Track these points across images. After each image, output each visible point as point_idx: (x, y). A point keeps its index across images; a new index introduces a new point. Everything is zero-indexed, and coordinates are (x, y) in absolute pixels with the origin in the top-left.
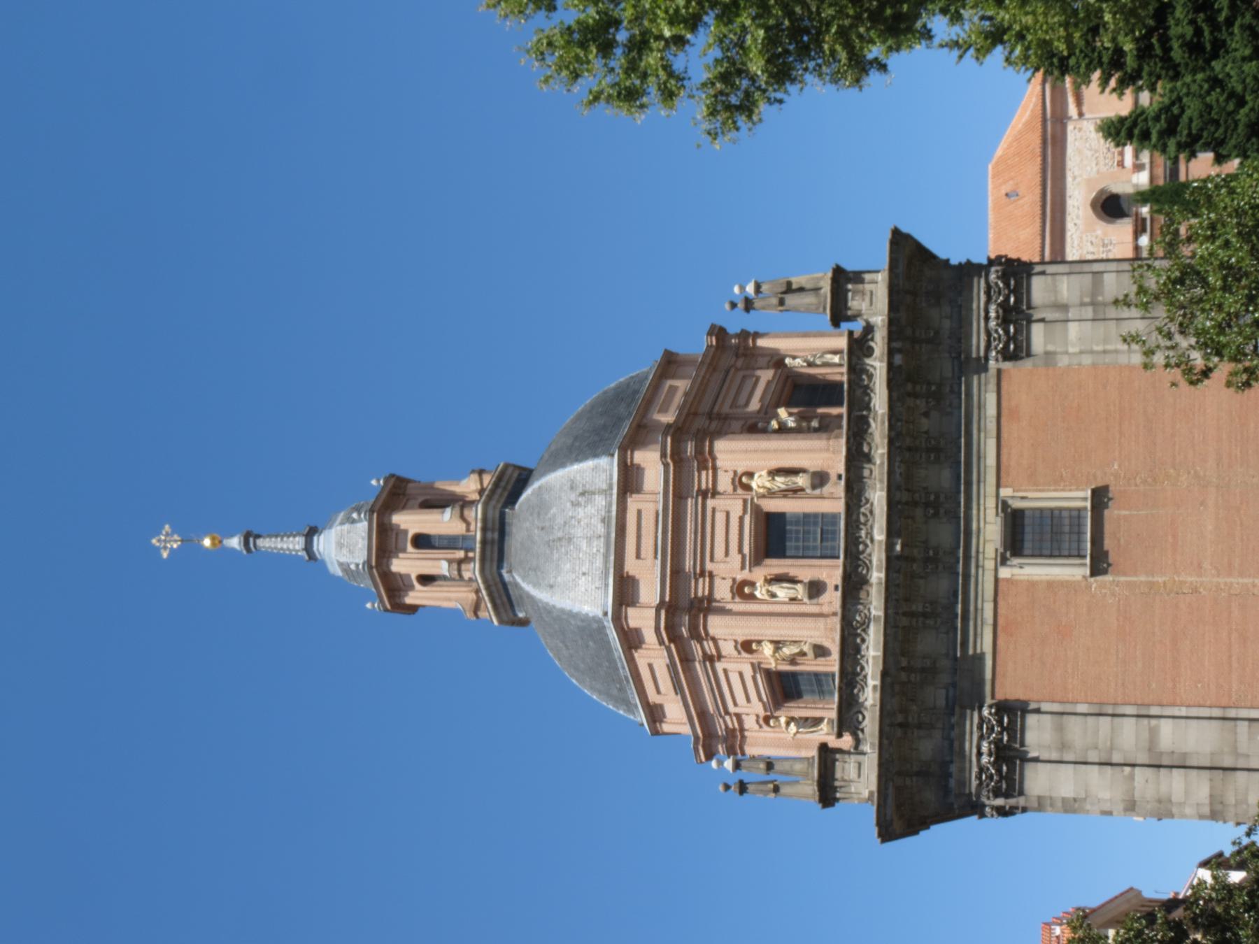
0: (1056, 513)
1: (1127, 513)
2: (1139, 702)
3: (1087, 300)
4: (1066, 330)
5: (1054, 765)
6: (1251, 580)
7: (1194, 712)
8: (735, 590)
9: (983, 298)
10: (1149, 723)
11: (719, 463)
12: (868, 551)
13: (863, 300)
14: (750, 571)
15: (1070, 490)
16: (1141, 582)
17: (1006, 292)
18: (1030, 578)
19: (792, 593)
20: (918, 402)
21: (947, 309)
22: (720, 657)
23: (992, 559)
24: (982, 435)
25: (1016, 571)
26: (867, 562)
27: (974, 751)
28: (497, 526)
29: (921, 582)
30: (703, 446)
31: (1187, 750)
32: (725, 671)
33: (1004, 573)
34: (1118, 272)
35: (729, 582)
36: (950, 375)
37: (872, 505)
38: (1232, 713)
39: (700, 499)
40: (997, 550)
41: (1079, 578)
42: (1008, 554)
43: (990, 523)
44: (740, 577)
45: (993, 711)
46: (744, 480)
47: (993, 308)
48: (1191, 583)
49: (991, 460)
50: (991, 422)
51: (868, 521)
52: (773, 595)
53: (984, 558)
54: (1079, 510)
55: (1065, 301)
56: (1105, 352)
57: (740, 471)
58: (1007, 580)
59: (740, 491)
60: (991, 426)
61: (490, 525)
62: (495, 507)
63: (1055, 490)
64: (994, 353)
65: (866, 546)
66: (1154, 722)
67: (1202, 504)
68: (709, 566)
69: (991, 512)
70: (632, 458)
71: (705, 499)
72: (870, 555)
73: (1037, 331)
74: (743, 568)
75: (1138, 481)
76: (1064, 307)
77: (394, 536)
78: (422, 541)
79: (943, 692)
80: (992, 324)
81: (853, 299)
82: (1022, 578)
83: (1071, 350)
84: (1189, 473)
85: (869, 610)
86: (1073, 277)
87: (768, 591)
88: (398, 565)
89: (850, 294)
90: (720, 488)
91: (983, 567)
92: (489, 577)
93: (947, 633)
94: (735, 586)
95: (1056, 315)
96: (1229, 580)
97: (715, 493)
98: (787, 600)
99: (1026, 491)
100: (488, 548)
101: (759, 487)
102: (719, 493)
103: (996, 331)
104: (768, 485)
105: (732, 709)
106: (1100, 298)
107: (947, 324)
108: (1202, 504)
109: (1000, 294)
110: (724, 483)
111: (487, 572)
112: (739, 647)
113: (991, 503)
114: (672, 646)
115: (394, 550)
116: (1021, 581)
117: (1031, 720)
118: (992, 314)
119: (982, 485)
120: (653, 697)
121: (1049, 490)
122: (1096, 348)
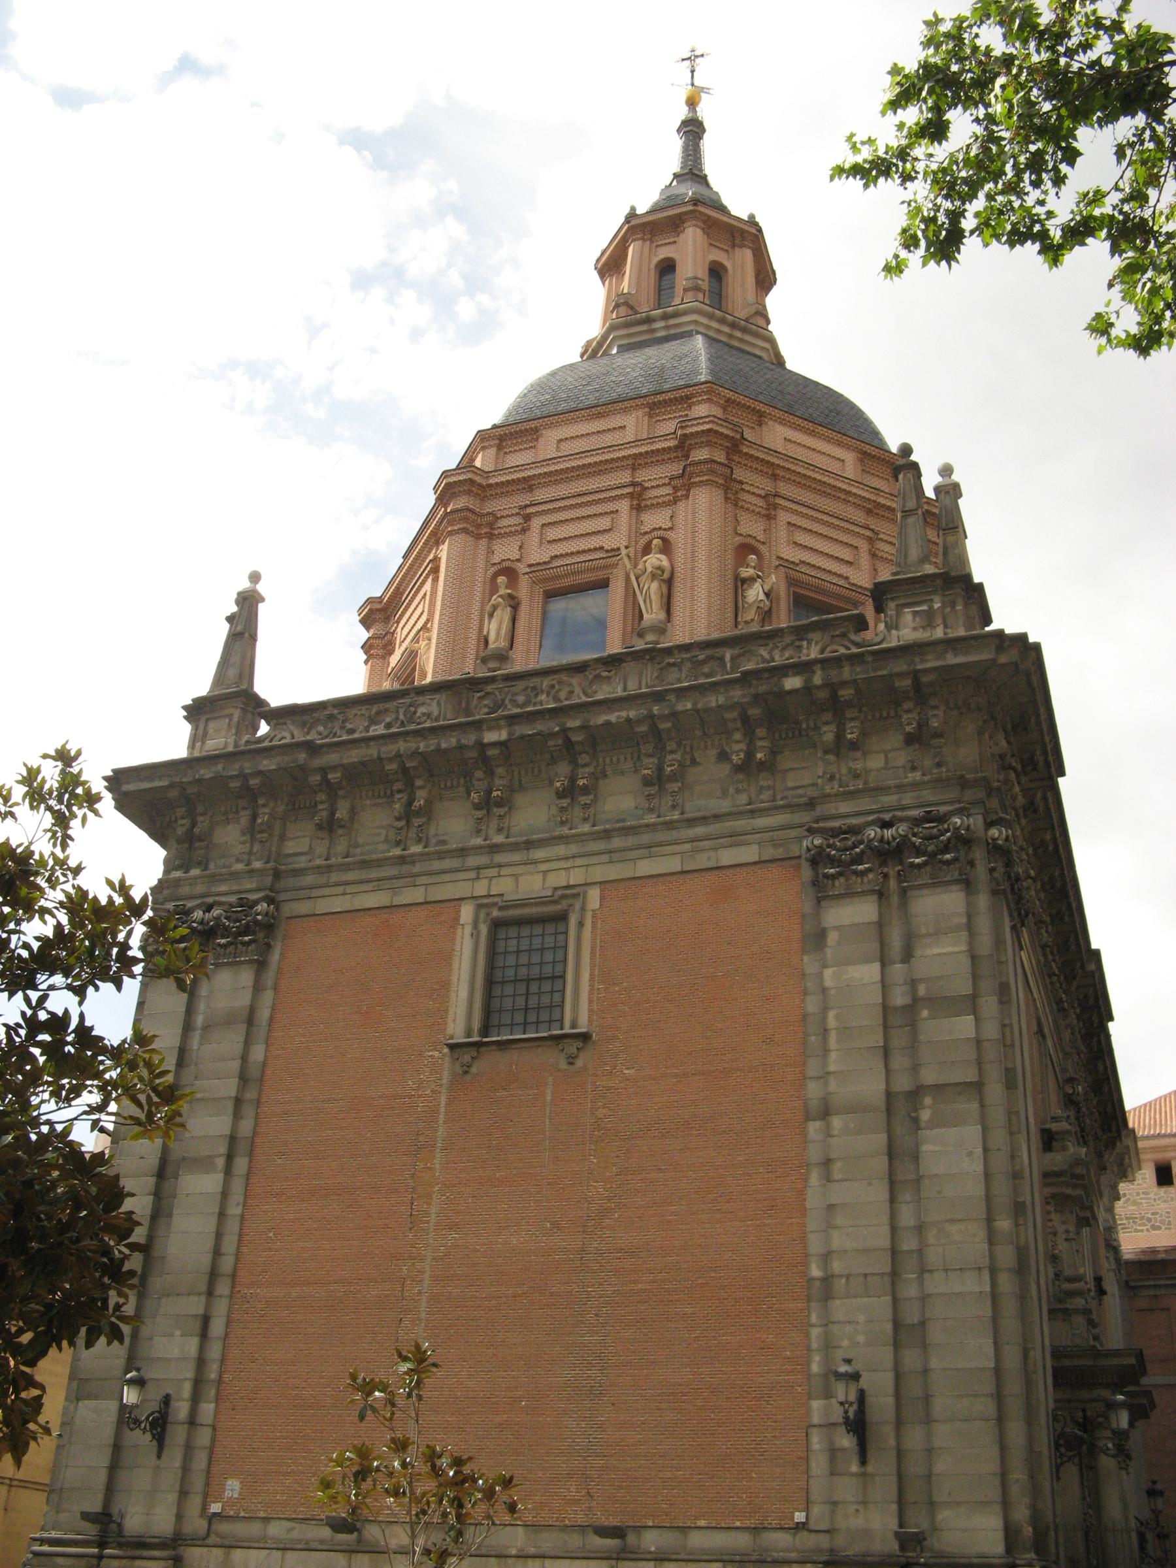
0: (558, 985)
1: (549, 1098)
2: (258, 1140)
3: (922, 990)
4: (866, 961)
5: (181, 1017)
6: (423, 1315)
7: (232, 1227)
8: (505, 564)
9: (915, 813)
10: (220, 1155)
11: (681, 505)
13: (914, 629)
15: (590, 1002)
16: (436, 1131)
17: (930, 849)
18: (457, 953)
19: (492, 637)
20: (738, 736)
21: (901, 758)
23: (489, 889)
24: (687, 847)
25: (468, 930)
27: (210, 900)
28: (672, 332)
29: (462, 789)
31: (174, 1218)
33: (467, 912)
34: (978, 1042)
36: (790, 784)
38: (223, 1288)
39: (630, 490)
40: (502, 895)
41: (450, 1031)
42: (495, 913)
43: (544, 880)
45: (259, 917)
46: (655, 542)
47: (902, 829)
48: (427, 1214)
49: (645, 867)
50: (709, 859)
52: (491, 615)
53: (491, 879)
54: (561, 1021)
55: (916, 955)
56: (825, 1031)
57: (671, 535)
58: (457, 918)
60: (703, 861)
61: (672, 322)
62: (696, 322)
63: (592, 979)
64: (817, 842)
66: (221, 1162)
67: (556, 1225)
68: (536, 523)
69: (558, 879)
70: (699, 402)
71: (631, 496)
73: (862, 911)
74: (530, 566)
75: (601, 1112)
76: (908, 955)
77: (672, 240)
79: (306, 849)
80: (871, 833)
81: (915, 613)
82: (458, 941)
83: (828, 973)
84: (609, 1199)
86: (966, 961)
89: (925, 608)
91: (478, 878)
93: (386, 840)
95: (896, 943)
96: (426, 1276)
97: (638, 509)
99: (594, 927)
100: (645, 327)
102: (638, 515)
103: (861, 842)
106: (925, 1013)
107: (875, 762)
108: (556, 1225)
109: (924, 838)
110: (655, 519)
113: (576, 877)
115: (655, 244)
116: (454, 939)
117: (246, 977)
118: (888, 833)
119: (605, 858)
121: (593, 966)
122: (831, 1014)
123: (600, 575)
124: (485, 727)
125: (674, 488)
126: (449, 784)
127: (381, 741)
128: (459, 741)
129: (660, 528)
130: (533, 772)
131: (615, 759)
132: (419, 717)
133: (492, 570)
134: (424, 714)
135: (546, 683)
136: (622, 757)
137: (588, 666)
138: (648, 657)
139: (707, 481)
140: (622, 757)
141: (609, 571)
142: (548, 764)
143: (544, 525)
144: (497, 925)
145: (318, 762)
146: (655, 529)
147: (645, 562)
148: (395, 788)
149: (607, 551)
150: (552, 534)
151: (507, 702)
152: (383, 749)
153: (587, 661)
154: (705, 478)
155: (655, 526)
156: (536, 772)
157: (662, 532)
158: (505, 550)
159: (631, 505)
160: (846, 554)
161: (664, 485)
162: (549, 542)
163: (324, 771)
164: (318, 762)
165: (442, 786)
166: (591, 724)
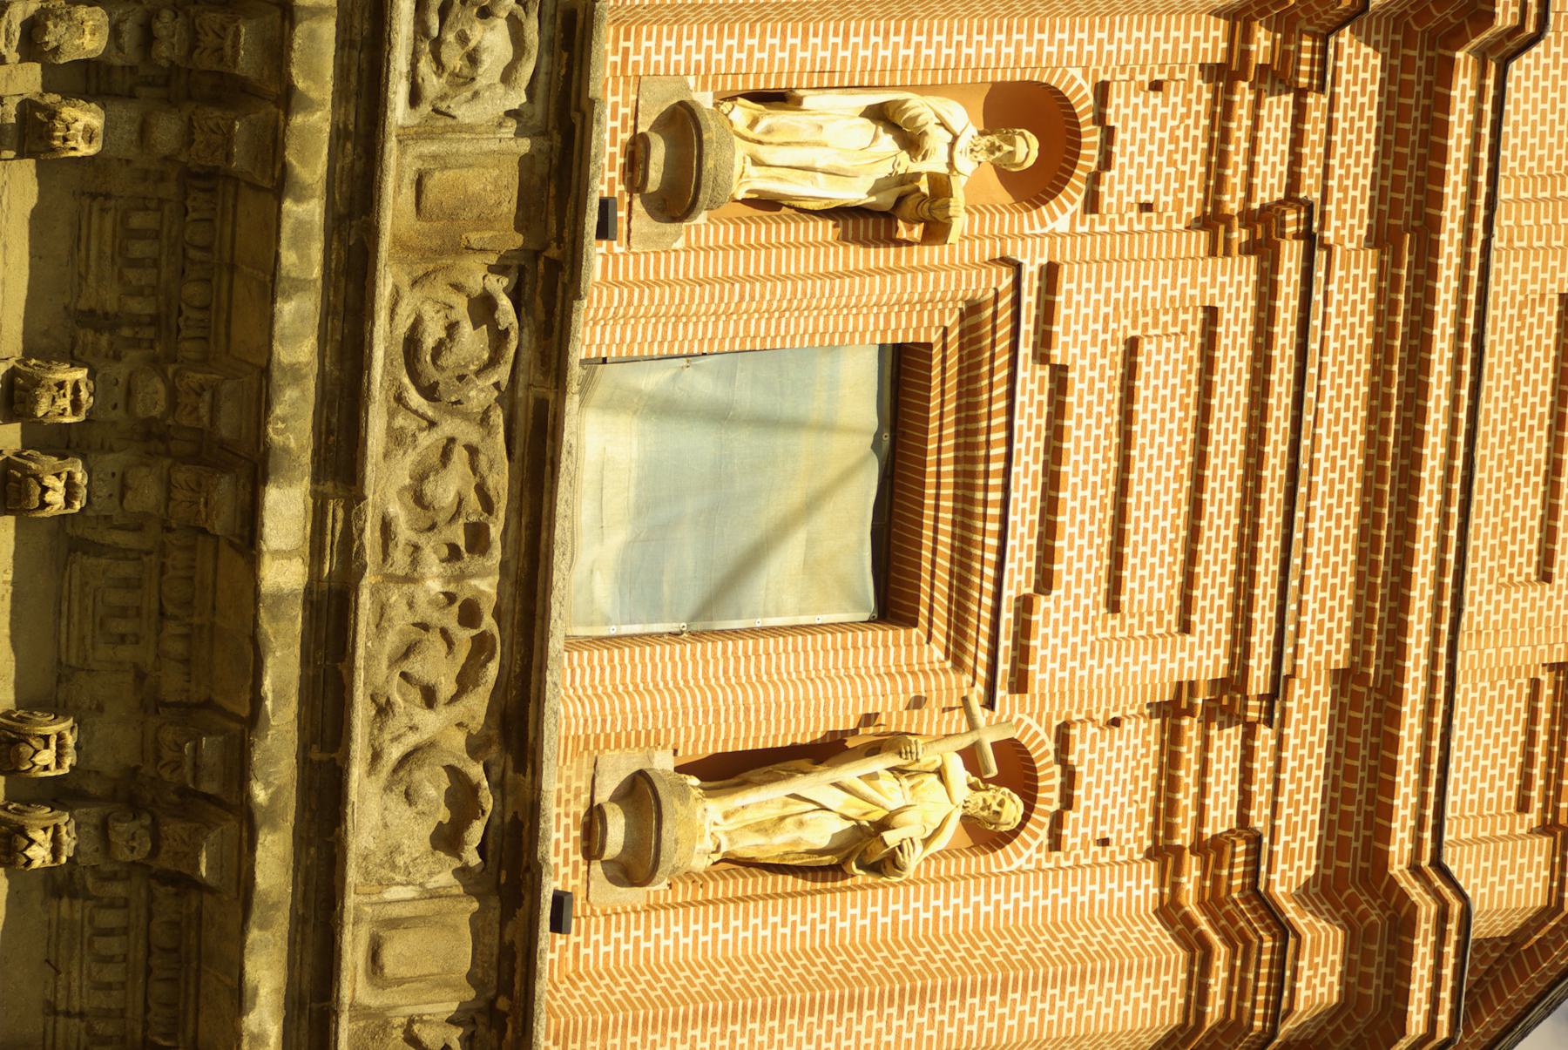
8: (1091, 138)
11: (1145, 886)
12: (402, 470)
14: (1018, 267)
26: (415, 399)
29: (109, 298)
30: (1238, 987)
35: (1116, 189)
37: (376, 756)
44: (1063, 214)
46: (1013, 809)
51: (394, 661)
52: (881, 115)
57: (1030, 850)
59: (1043, 749)
65: (419, 499)
72: (397, 438)
74: (1050, 273)
85: (415, 98)
87: (912, 142)
90: (1141, 738)
94: (1089, 157)
97: (1170, 711)
98: (811, 100)
101: (940, 773)
104: (891, 793)
123: (935, 591)
124: (328, 487)
125: (1218, 843)
126: (139, 249)
127: (362, 27)
128: (295, 374)
129: (1068, 801)
130: (123, 613)
131: (114, 946)
132: (463, 39)
134: (473, 58)
135: (486, 586)
136: (111, 974)
137: (520, 767)
138: (503, 1004)
139: (1201, 1016)
140: (111, 974)
141: (940, 624)
142: (140, 676)
143: (1212, 314)
146: (1069, 777)
147: (940, 773)
148: (166, 24)
149: (1025, 605)
151: (449, 427)
152: (328, 30)
153: (537, 772)
154: (1214, 1010)
155: (1084, 779)
156: (122, 626)
157: (1056, 806)
159: (1192, 685)
161: (1245, 800)
162: (1132, 345)
165: (137, 221)
166: (254, 934)
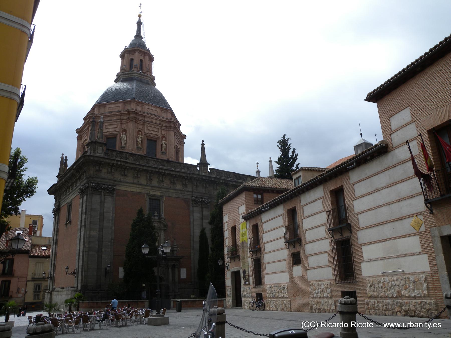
14: (144, 135)
22: (122, 123)
32: (118, 124)
39: (161, 126)
42: (150, 197)
57: (166, 136)
61: (146, 77)
62: (149, 79)
68: (146, 125)
71: (161, 127)
78: (141, 61)
88: (137, 54)
92: (134, 74)
100: (140, 76)
105: (104, 125)
110: (164, 133)
111: (136, 74)
112: (124, 129)
114: (127, 112)
120: (108, 106)
133: (138, 130)
144: (150, 199)
145: (126, 165)
150: (149, 128)
158: (140, 127)
160: (178, 142)
163: (126, 167)
164: (126, 165)
